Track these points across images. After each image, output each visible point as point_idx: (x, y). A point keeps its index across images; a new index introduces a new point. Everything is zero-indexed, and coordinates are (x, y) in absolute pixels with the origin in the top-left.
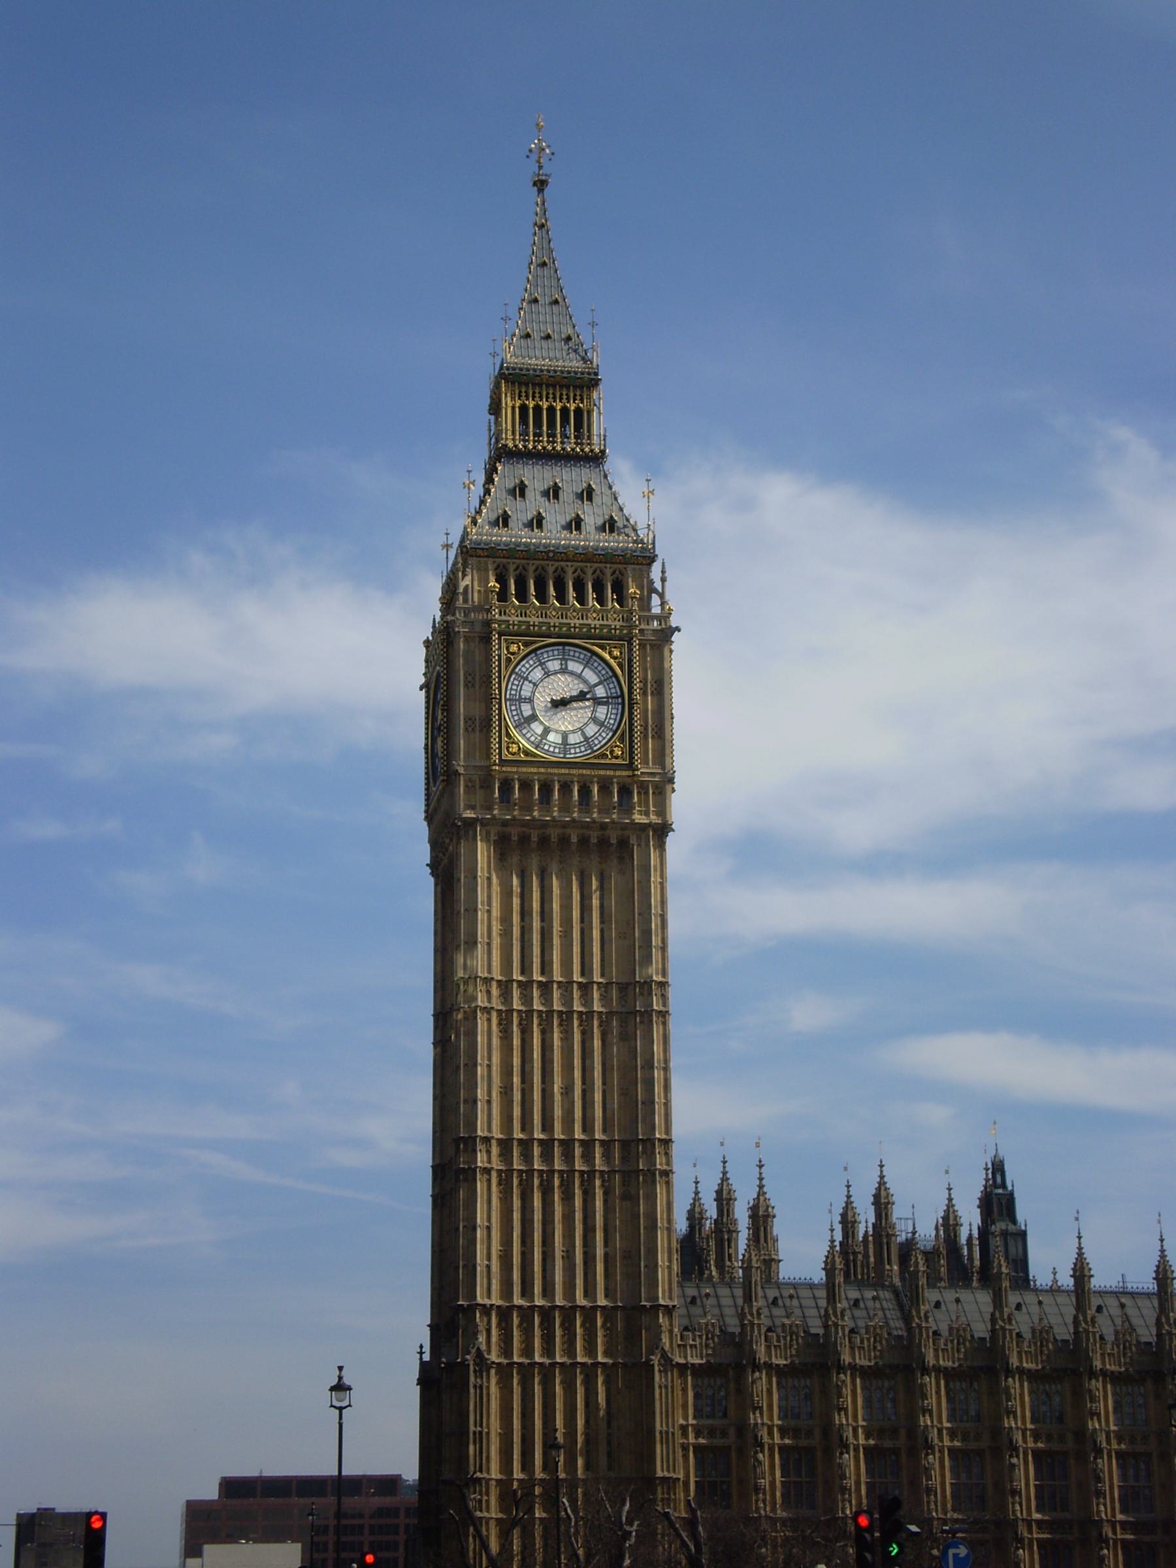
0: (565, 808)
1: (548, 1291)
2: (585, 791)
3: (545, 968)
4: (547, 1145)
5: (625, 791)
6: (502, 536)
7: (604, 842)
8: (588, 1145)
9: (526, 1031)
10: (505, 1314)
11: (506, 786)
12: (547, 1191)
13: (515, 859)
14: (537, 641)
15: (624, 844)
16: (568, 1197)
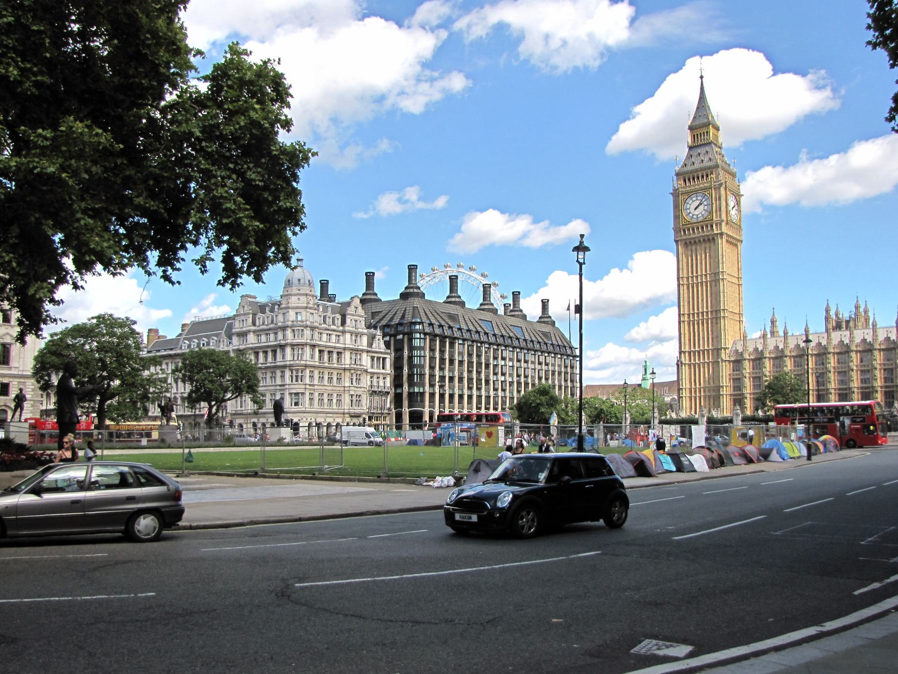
0: (699, 232)
1: (699, 347)
2: (702, 228)
3: (697, 272)
4: (698, 314)
5: (712, 226)
6: (685, 169)
7: (709, 239)
8: (707, 312)
9: (693, 288)
10: (690, 353)
11: (684, 231)
12: (698, 324)
13: (689, 248)
14: (689, 194)
15: (713, 239)
16: (703, 325)
